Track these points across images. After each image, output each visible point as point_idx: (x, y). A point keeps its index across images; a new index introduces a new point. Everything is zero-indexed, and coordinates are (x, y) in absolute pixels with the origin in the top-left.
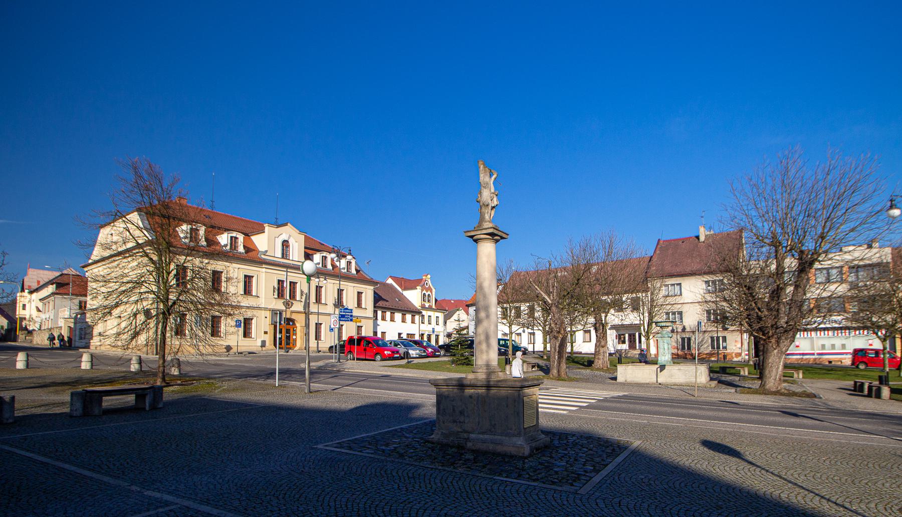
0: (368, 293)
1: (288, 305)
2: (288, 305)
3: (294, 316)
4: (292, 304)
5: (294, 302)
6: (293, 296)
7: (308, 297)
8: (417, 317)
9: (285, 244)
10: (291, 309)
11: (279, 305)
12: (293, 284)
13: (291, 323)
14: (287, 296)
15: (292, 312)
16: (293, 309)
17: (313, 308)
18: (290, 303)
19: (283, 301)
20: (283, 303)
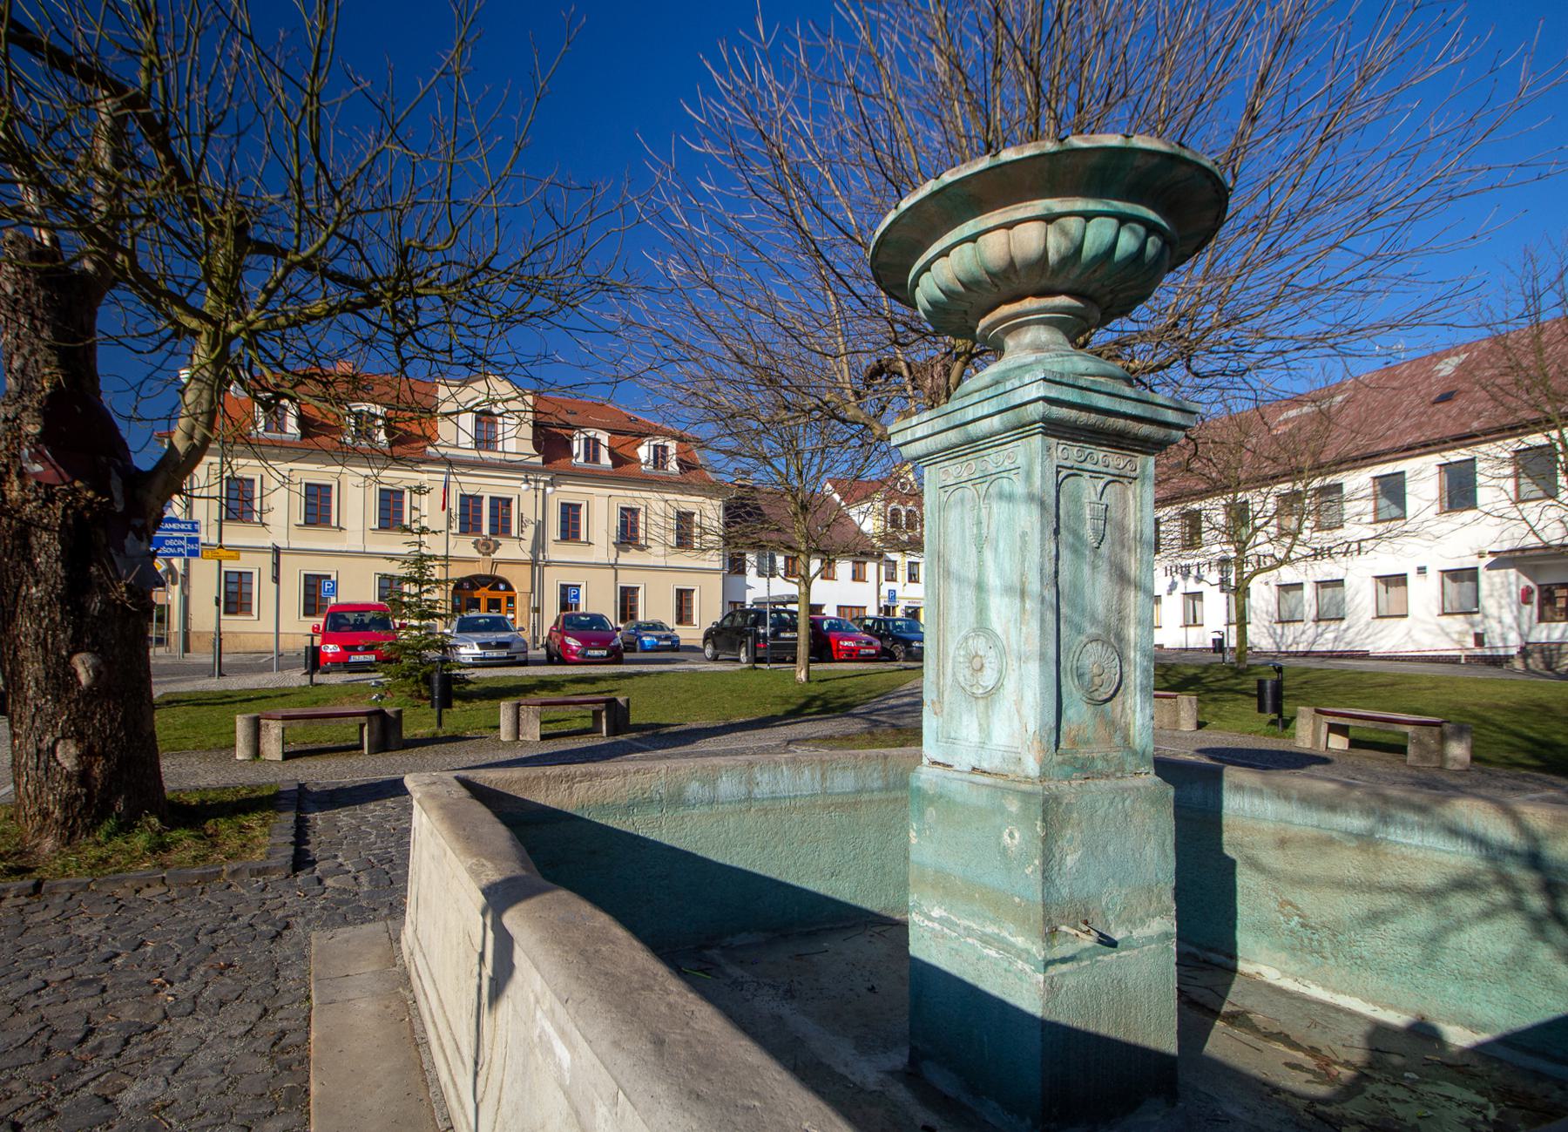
0: (709, 512)
1: (487, 547)
2: (487, 547)
3: (501, 572)
4: (497, 545)
5: (501, 540)
6: (501, 526)
7: (541, 528)
8: (871, 568)
9: (485, 418)
10: (493, 556)
11: (464, 547)
12: (501, 506)
13: (502, 587)
14: (486, 530)
15: (495, 563)
16: (498, 555)
17: (556, 551)
18: (491, 543)
19: (473, 539)
20: (476, 544)
